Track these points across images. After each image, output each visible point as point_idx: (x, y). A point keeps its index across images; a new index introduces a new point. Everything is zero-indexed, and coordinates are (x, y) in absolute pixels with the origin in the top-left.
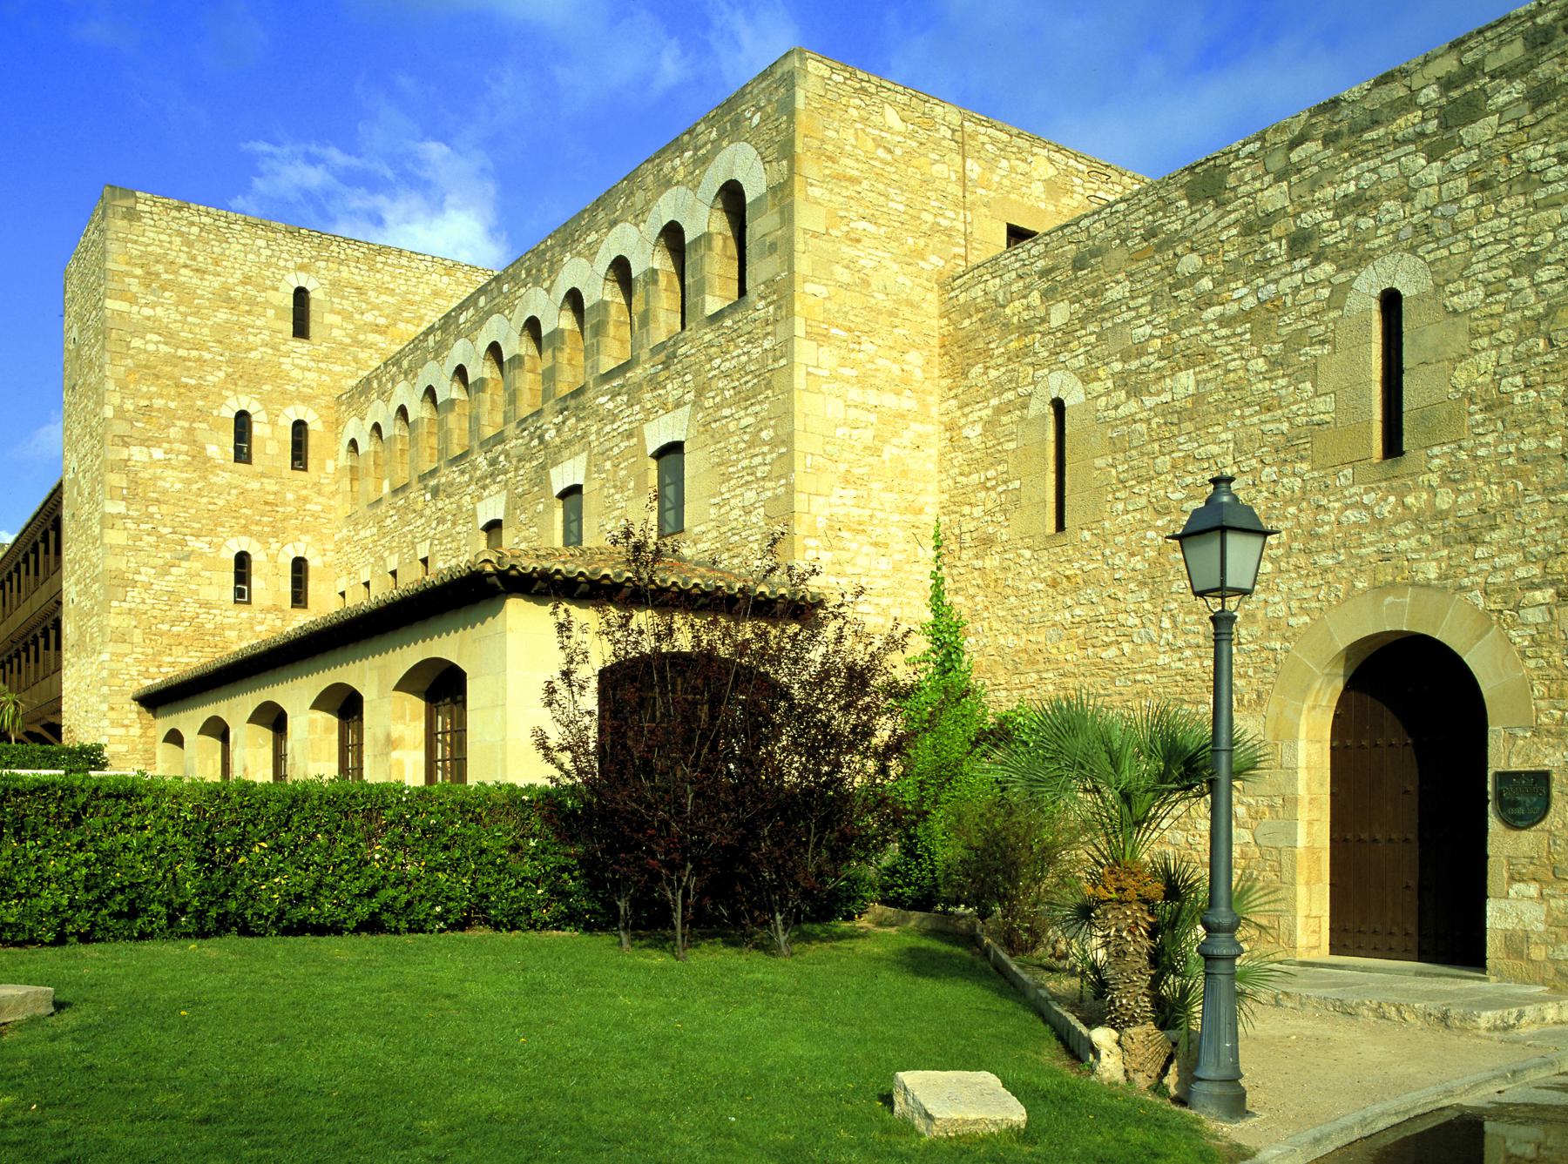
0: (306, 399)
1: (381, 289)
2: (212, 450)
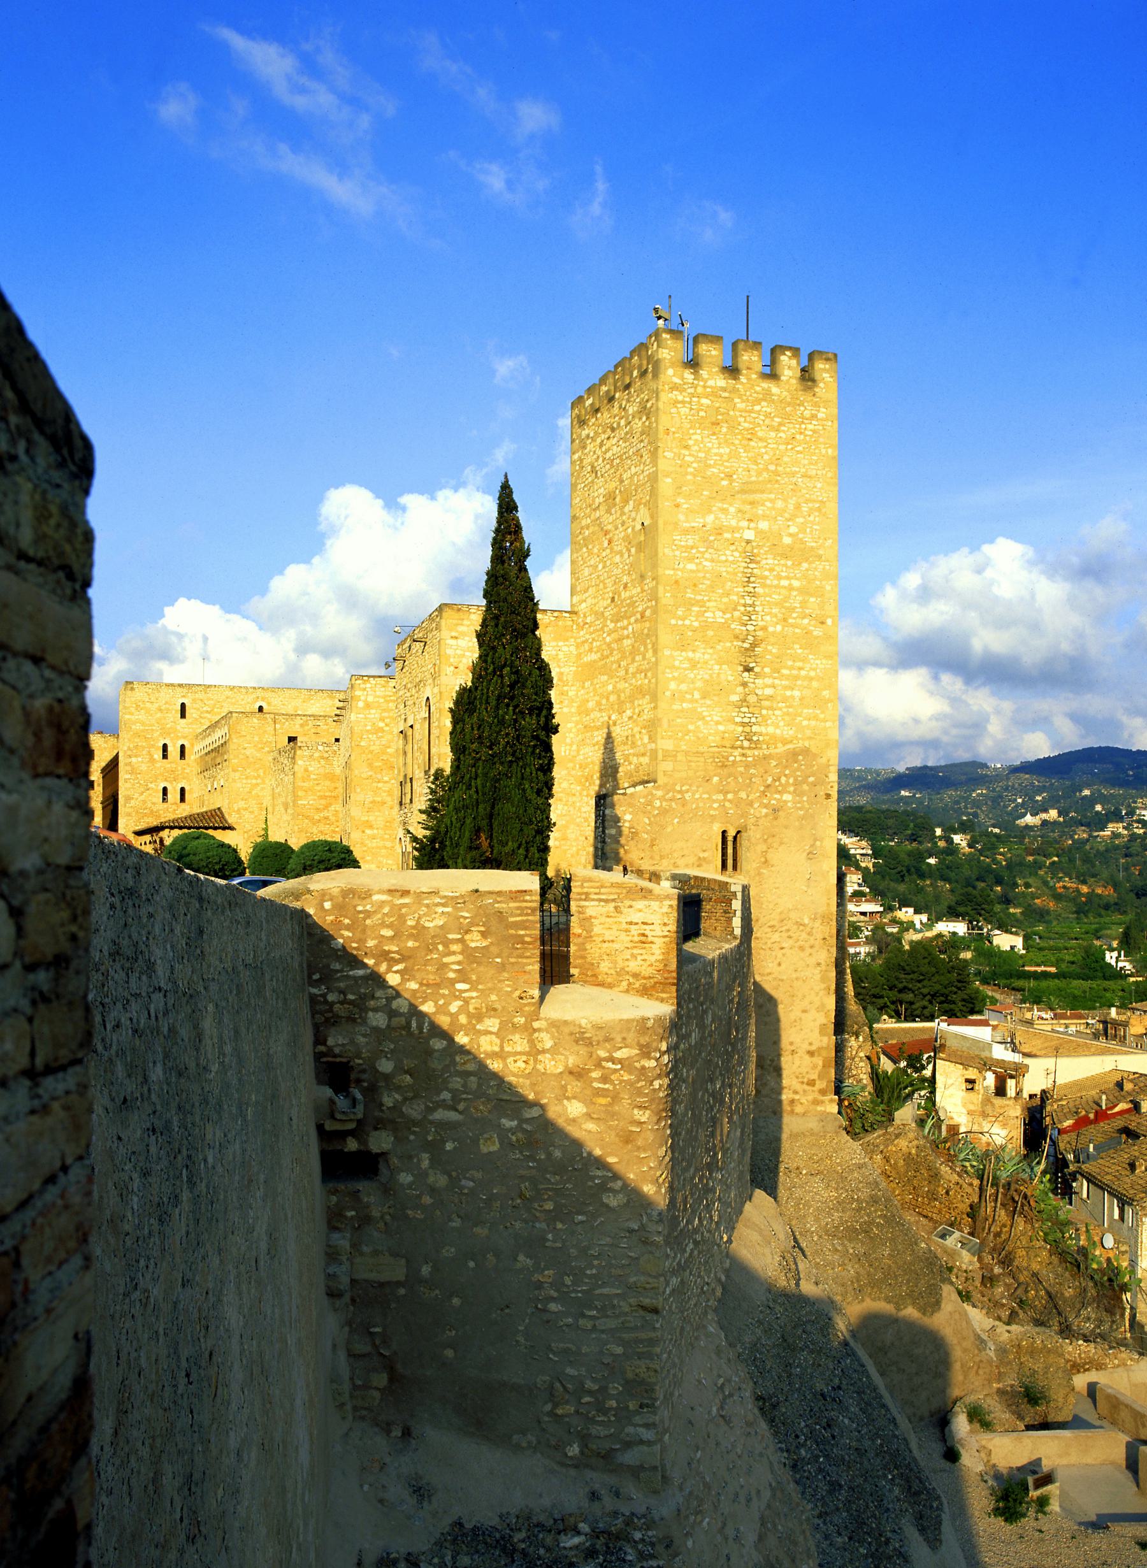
0: (184, 737)
1: (209, 699)
2: (156, 756)
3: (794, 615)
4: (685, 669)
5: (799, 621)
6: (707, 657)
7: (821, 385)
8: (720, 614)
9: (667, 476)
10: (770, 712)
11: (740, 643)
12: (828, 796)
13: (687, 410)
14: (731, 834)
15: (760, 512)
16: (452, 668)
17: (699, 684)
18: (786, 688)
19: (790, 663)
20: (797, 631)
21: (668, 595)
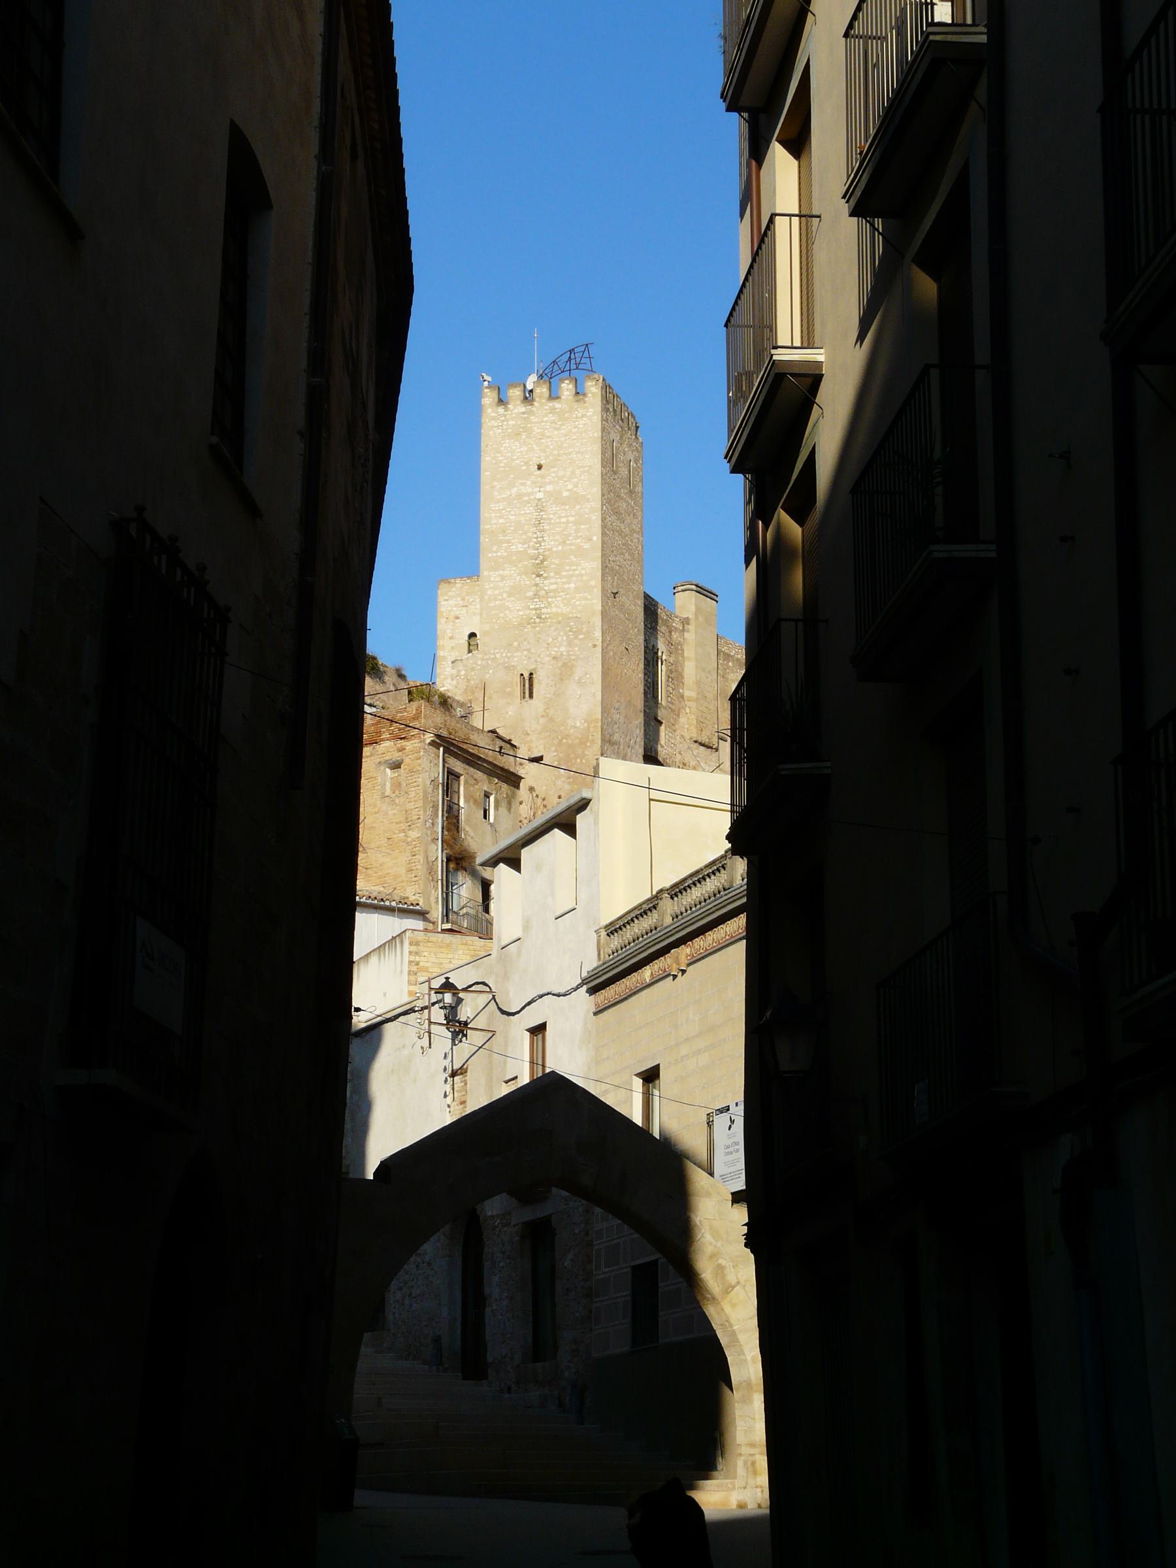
3: (571, 538)
4: (498, 582)
5: (574, 541)
6: (513, 572)
7: (590, 395)
8: (521, 545)
9: (487, 471)
10: (554, 599)
11: (534, 561)
12: (595, 646)
13: (500, 431)
14: (526, 676)
15: (547, 480)
16: (445, 619)
17: (507, 589)
18: (564, 583)
19: (567, 568)
20: (572, 547)
21: (487, 540)
